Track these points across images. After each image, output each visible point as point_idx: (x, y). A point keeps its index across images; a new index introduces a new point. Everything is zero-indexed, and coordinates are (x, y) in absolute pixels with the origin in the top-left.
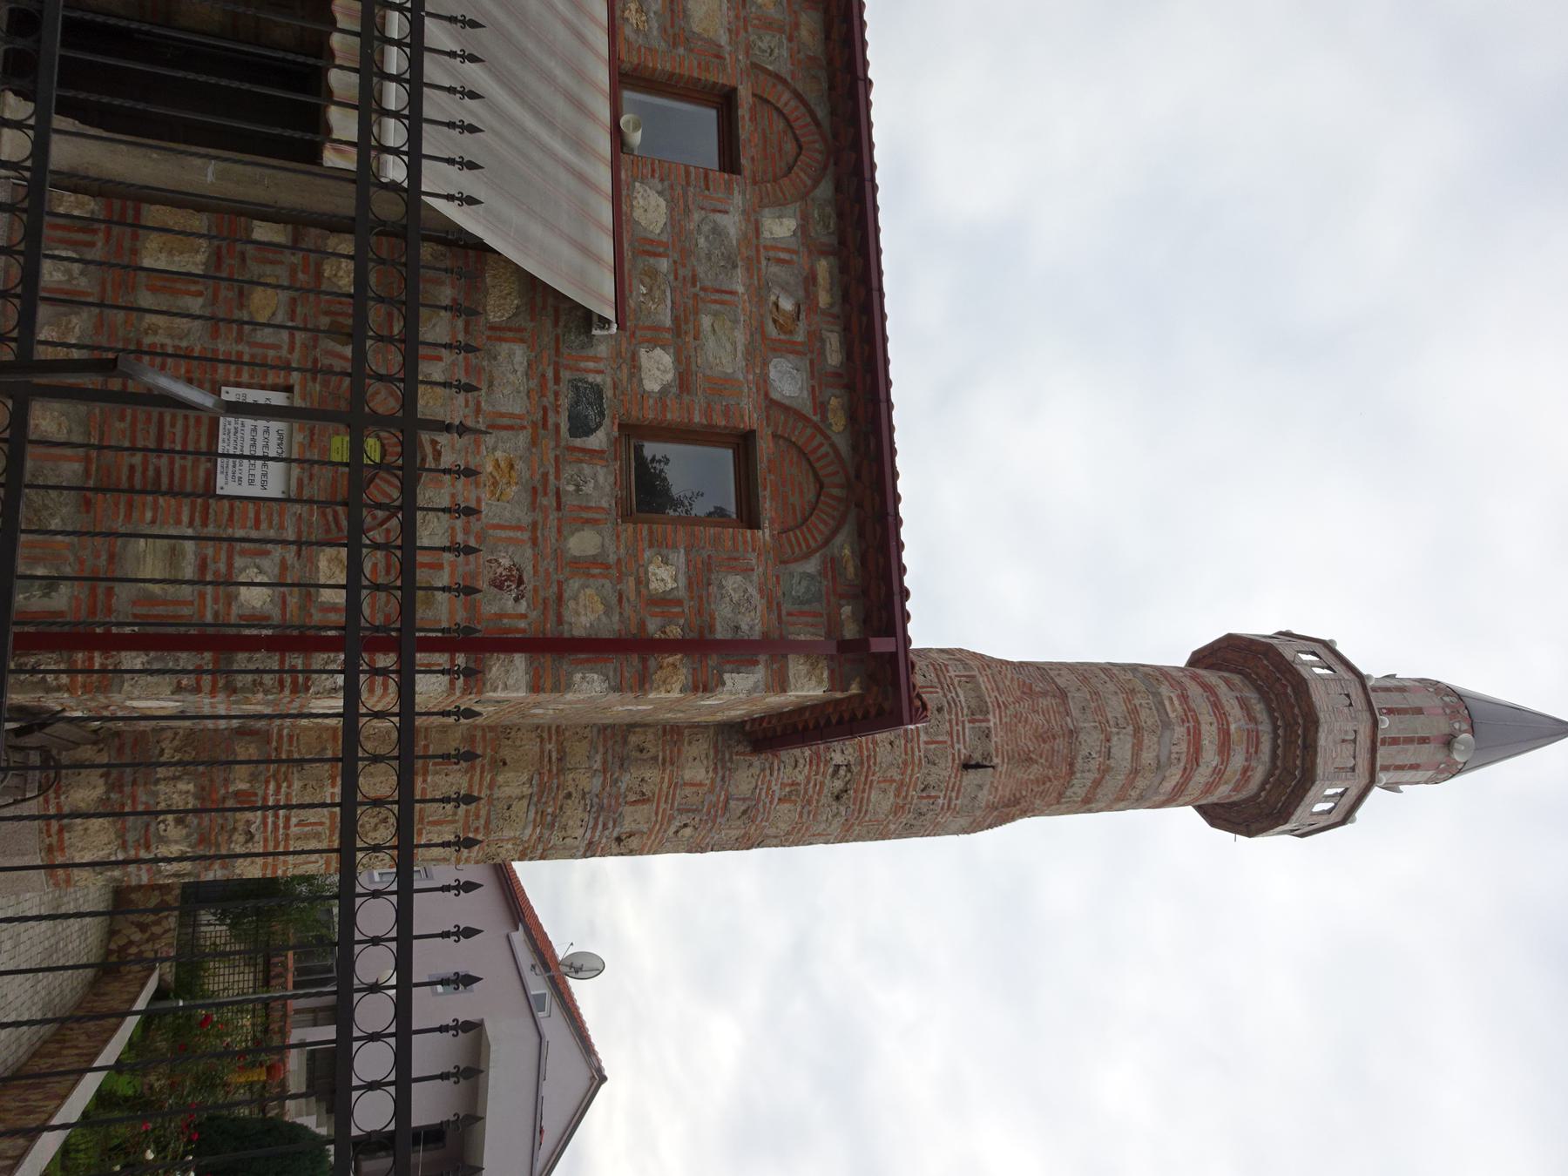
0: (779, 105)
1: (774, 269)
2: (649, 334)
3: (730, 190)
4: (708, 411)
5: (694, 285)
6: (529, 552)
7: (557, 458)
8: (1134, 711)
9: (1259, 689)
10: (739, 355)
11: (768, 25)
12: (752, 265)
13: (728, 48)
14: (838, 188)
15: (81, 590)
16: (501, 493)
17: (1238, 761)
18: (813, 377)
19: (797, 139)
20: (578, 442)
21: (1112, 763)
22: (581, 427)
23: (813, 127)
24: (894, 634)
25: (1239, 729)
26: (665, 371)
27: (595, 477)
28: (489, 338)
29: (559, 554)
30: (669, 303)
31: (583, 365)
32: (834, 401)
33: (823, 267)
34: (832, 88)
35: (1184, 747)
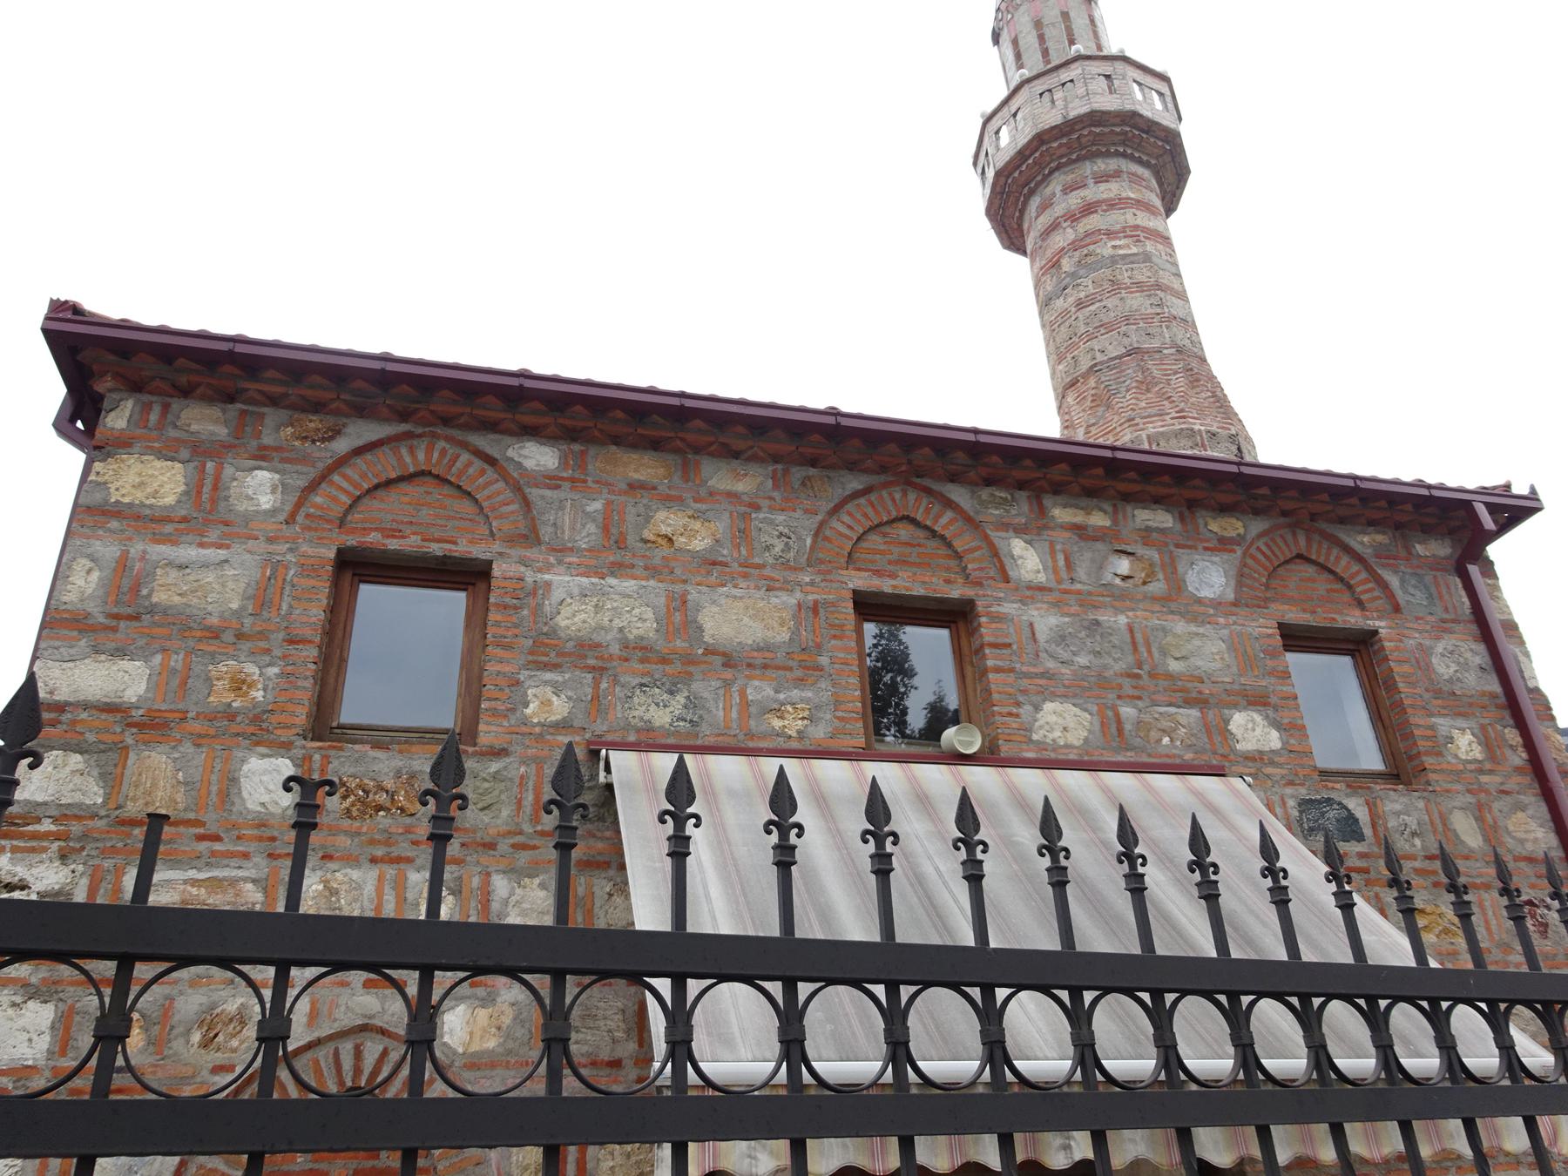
1: (1081, 573)
3: (998, 618)
5: (1138, 676)
8: (1140, 286)
10: (1201, 630)
11: (742, 534)
12: (1086, 601)
14: (953, 478)
20: (1368, 832)
23: (873, 497)
24: (1469, 503)
26: (1253, 721)
27: (1398, 814)
30: (1172, 710)
33: (1061, 514)
34: (813, 462)
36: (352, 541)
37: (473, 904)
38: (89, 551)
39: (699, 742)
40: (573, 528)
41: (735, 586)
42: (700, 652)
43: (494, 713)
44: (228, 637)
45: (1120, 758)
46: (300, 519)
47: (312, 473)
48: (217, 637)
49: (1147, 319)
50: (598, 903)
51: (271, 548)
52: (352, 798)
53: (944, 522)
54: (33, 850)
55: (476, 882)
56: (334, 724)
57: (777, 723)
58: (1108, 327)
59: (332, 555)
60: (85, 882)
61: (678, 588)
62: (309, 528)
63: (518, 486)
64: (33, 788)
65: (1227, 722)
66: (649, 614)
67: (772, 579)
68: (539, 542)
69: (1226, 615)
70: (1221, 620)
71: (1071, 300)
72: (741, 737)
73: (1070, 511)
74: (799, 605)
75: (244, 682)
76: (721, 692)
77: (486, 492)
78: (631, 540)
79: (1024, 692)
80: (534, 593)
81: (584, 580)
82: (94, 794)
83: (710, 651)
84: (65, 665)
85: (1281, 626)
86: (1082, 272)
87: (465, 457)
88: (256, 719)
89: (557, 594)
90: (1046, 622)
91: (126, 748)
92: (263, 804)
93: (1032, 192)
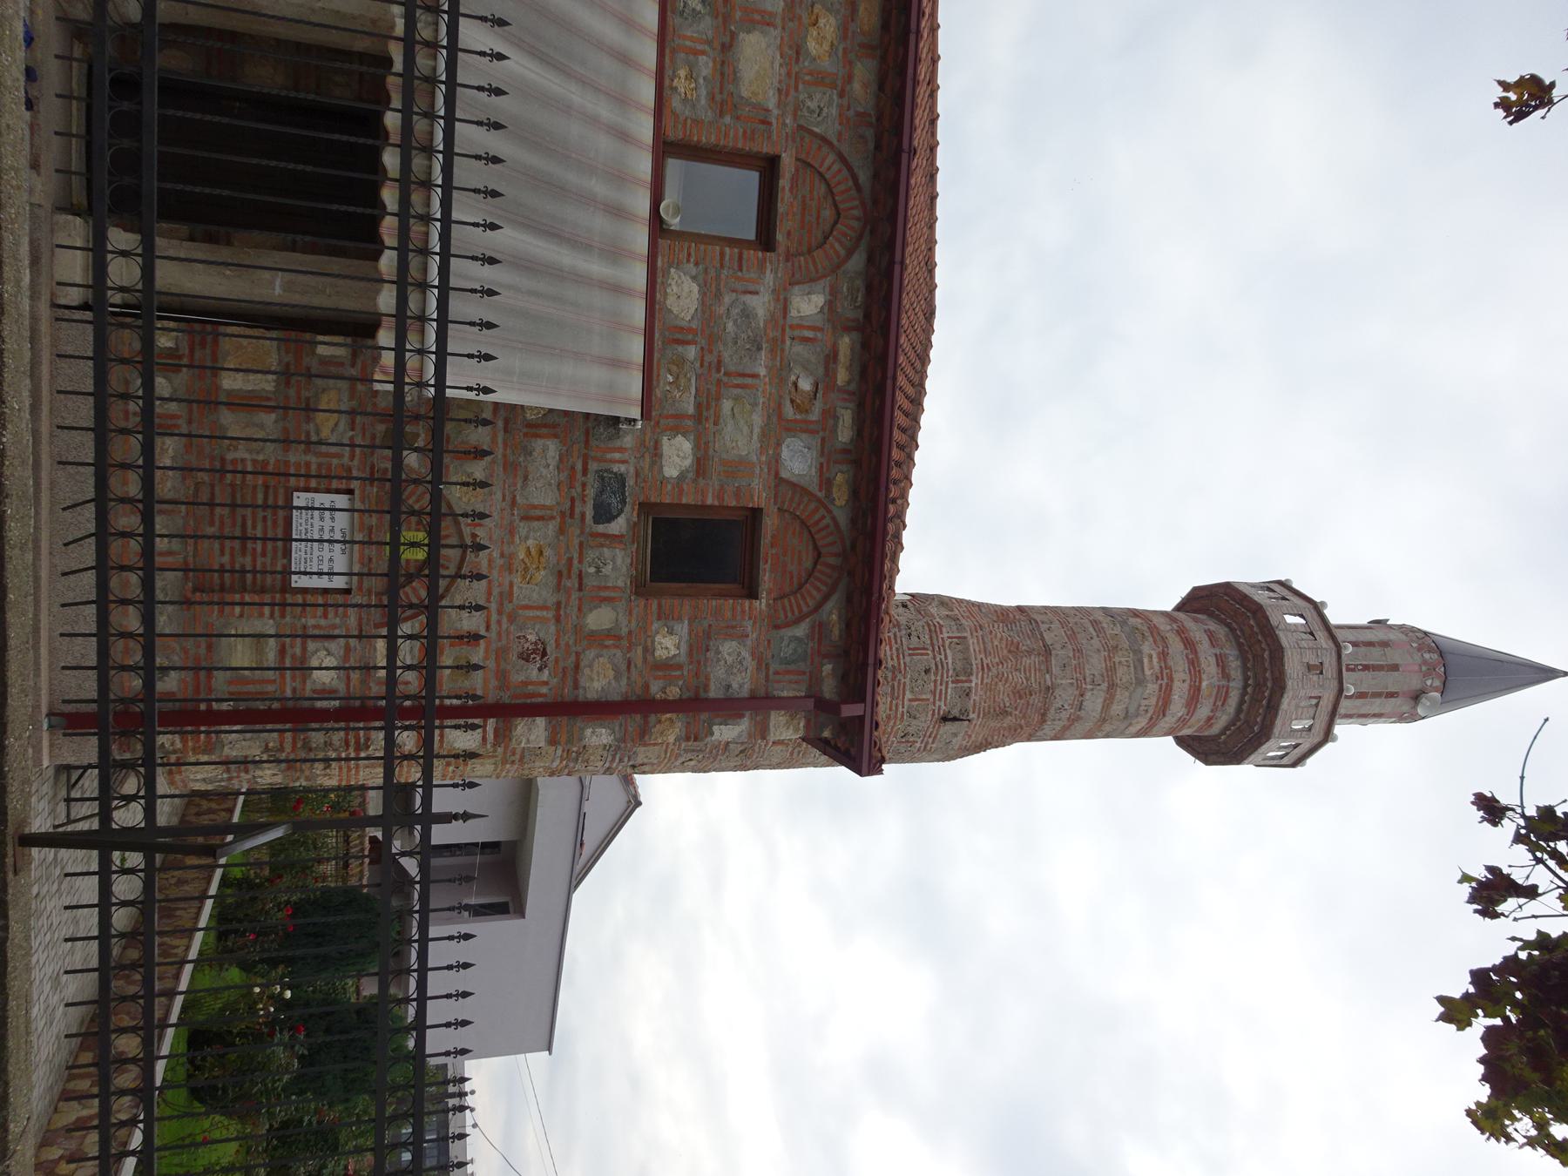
0: (822, 170)
1: (799, 348)
2: (671, 422)
4: (720, 497)
5: (718, 371)
6: (553, 629)
7: (581, 544)
8: (1111, 670)
9: (1240, 646)
11: (820, 79)
12: (776, 346)
13: (776, 112)
14: (870, 260)
15: (188, 676)
16: (529, 580)
17: (1204, 711)
18: (822, 453)
19: (835, 204)
20: (601, 528)
21: (1082, 713)
22: (604, 514)
23: (853, 192)
24: (863, 700)
25: (1210, 685)
26: (685, 458)
27: (613, 560)
28: (526, 435)
29: (578, 629)
30: (693, 391)
31: (609, 456)
32: (839, 478)
33: (845, 343)
34: (878, 147)
35: (1153, 701)
49: (1079, 668)
53: (836, 247)
57: (682, 73)
61: (779, 22)
69: (769, 463)
74: (767, 110)
83: (733, 35)
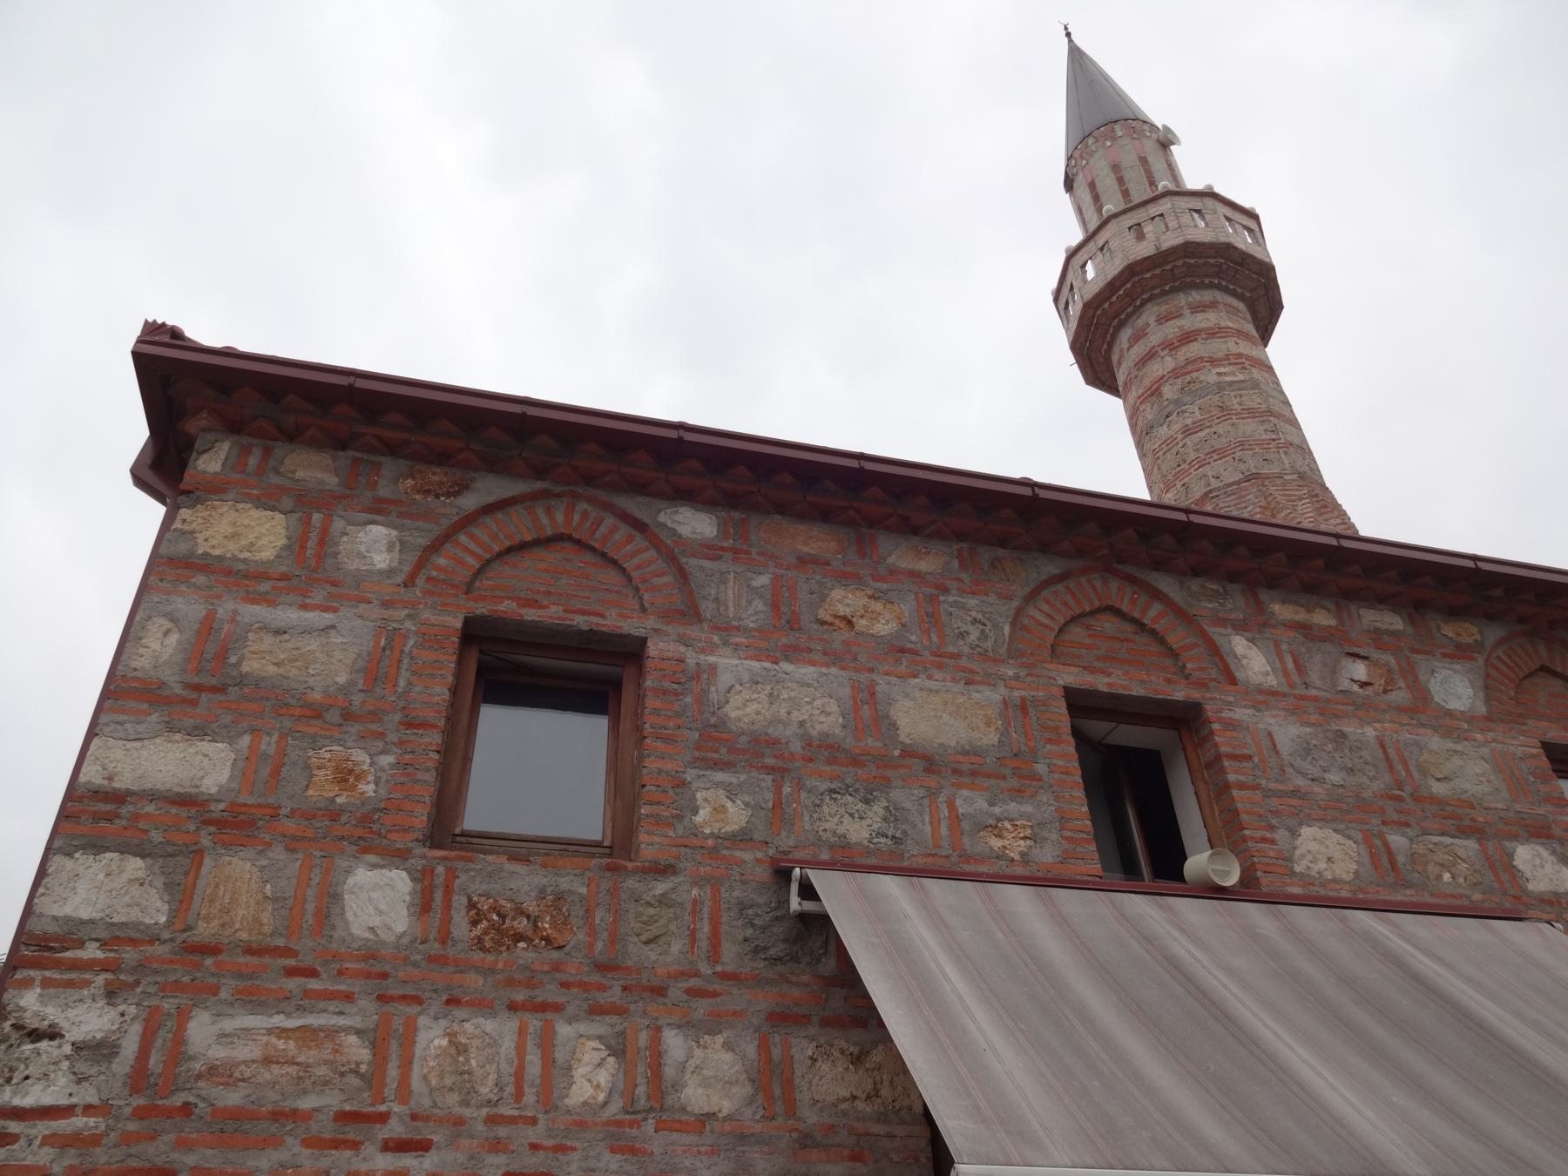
1: (1314, 677)
3: (1231, 725)
5: (1399, 799)
8: (1251, 413)
9: (1173, 290)
10: (1459, 747)
11: (931, 619)
14: (1158, 566)
19: (1093, 613)
23: (1071, 583)
26: (1539, 855)
30: (1447, 840)
33: (1282, 611)
34: (1002, 542)
36: (481, 609)
37: (641, 1069)
38: (168, 609)
39: (905, 864)
40: (737, 605)
41: (930, 677)
42: (897, 753)
43: (658, 821)
44: (333, 716)
45: (1399, 897)
46: (420, 582)
47: (436, 530)
48: (319, 716)
50: (798, 1072)
51: (386, 613)
52: (485, 924)
53: (1152, 613)
54: (71, 984)
55: (643, 1038)
56: (458, 831)
57: (996, 843)
58: (1222, 453)
59: (459, 624)
60: (136, 1029)
61: (864, 677)
62: (431, 593)
63: (672, 554)
64: (78, 900)
65: (1511, 856)
66: (833, 707)
67: (971, 671)
68: (698, 617)
69: (1482, 730)
70: (1479, 736)
71: (1176, 427)
72: (954, 859)
73: (1291, 608)
74: (1005, 702)
75: (351, 772)
76: (926, 802)
77: (636, 561)
78: (805, 619)
79: (1276, 813)
80: (697, 677)
81: (755, 664)
82: (155, 910)
83: (908, 753)
84: (129, 745)
85: (1547, 747)
86: (1186, 399)
87: (610, 521)
88: (365, 820)
89: (724, 680)
90: (1287, 732)
91: (200, 853)
92: (372, 929)
93: (1122, 324)
